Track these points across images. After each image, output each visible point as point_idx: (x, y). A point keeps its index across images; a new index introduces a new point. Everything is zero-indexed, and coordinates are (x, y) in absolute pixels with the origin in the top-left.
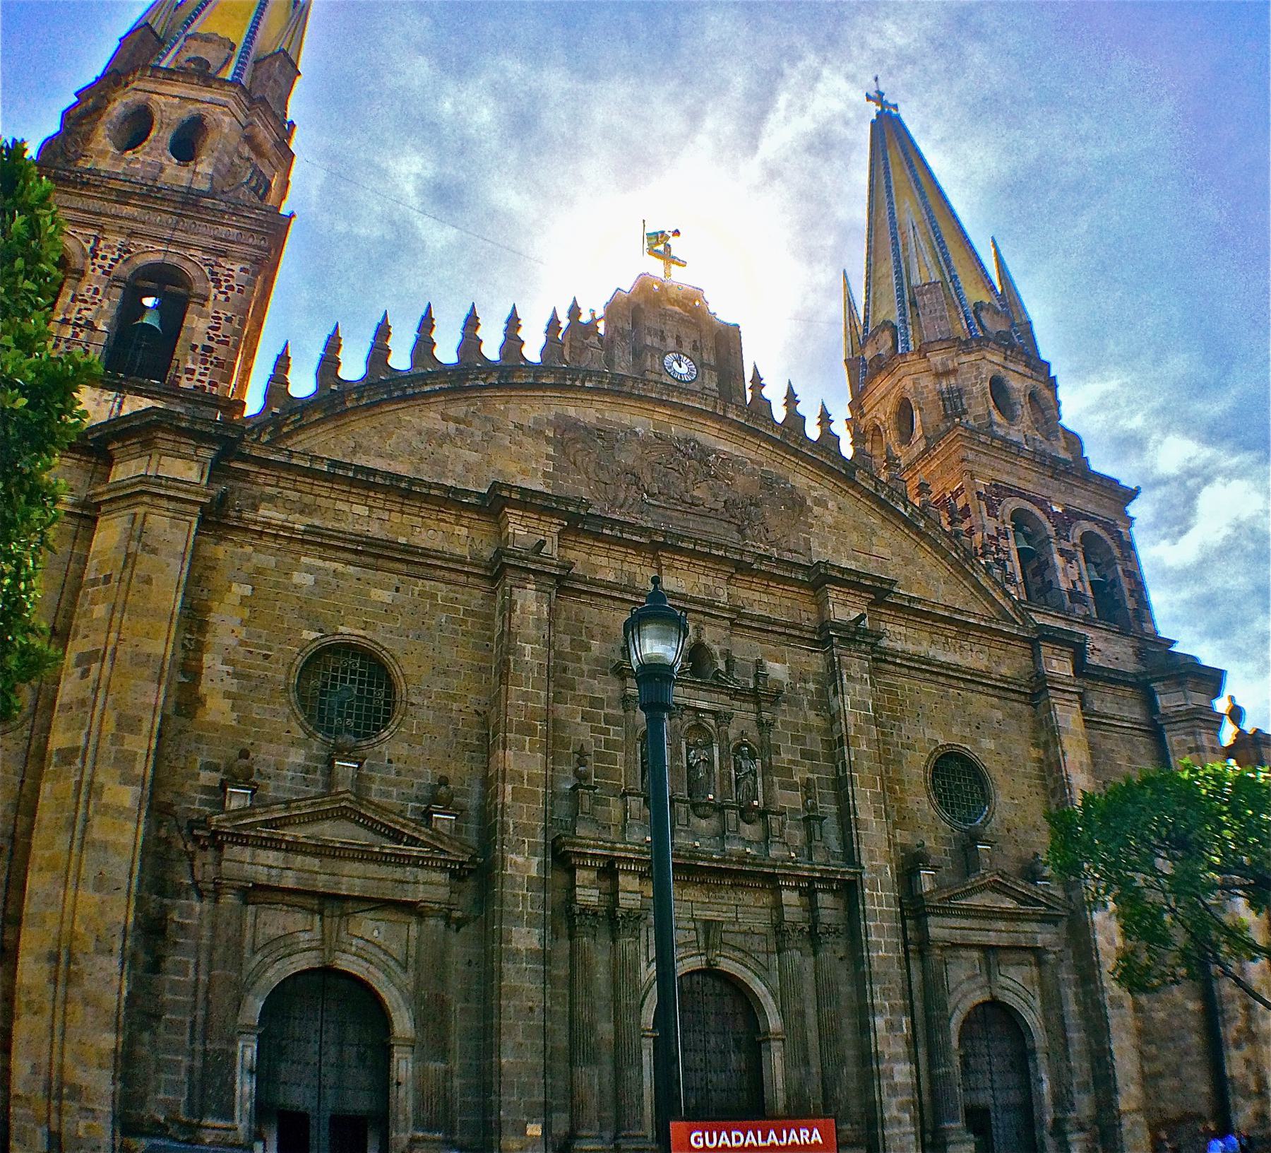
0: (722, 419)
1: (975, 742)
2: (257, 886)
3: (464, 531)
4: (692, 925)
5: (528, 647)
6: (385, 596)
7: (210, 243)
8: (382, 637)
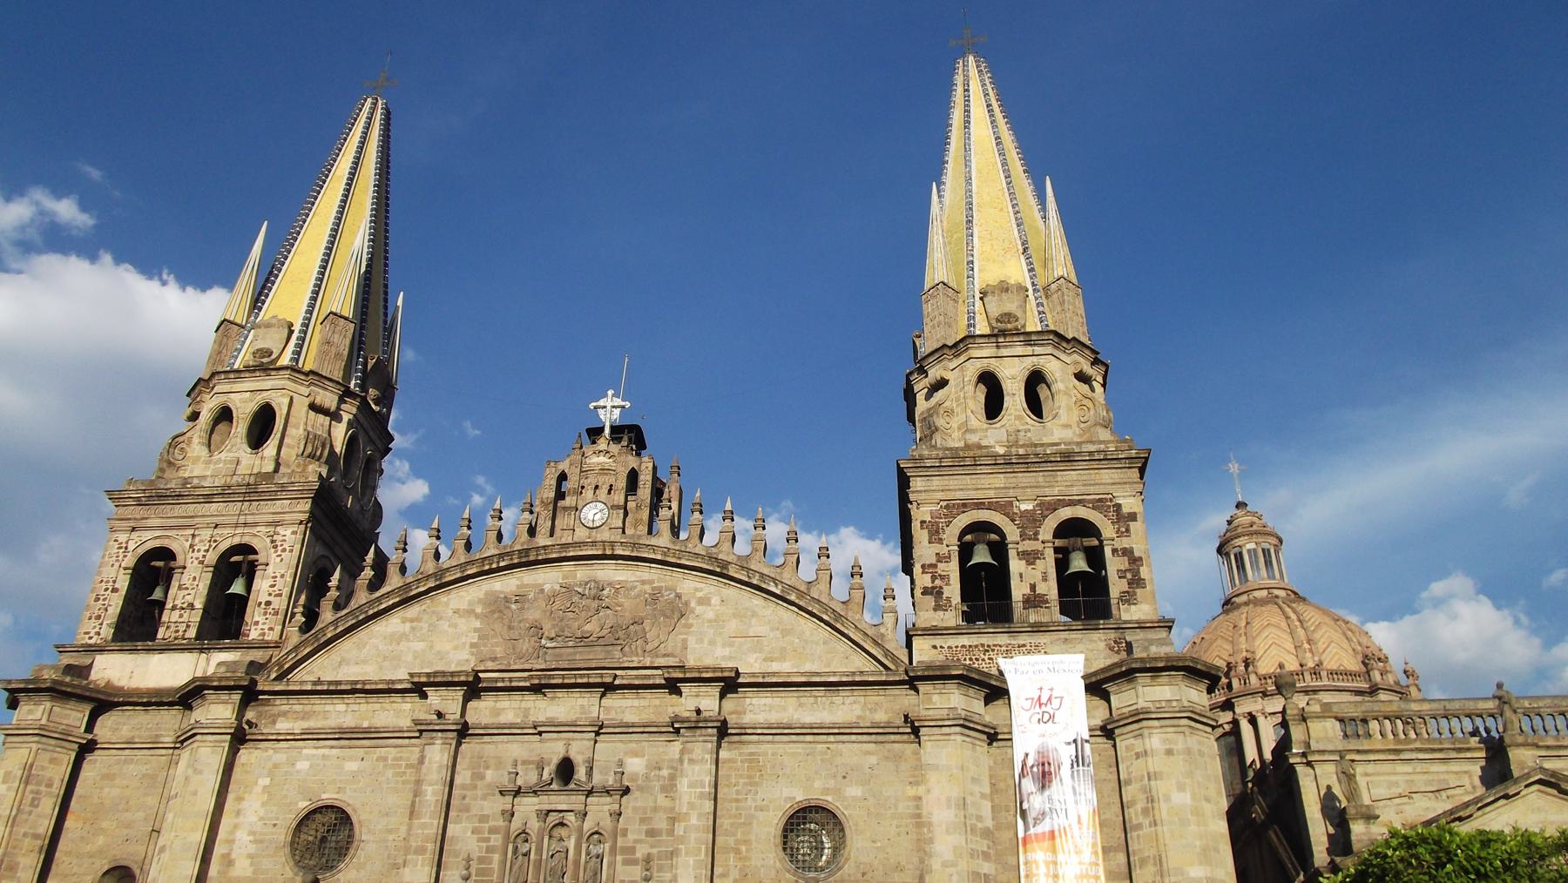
1: (837, 791)
5: (430, 789)
6: (352, 766)
7: (270, 518)
8: (348, 799)
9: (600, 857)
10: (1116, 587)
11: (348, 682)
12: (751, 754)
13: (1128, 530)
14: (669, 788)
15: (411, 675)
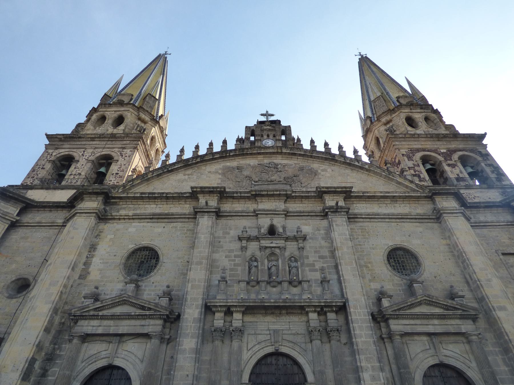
0: (281, 153)
2: (88, 335)
3: (188, 206)
4: (268, 332)
5: (203, 236)
6: (160, 230)
7: (120, 146)
8: (157, 243)
9: (297, 268)
10: (493, 176)
11: (159, 193)
12: (361, 226)
13: (487, 159)
14: (328, 236)
15: (192, 188)
